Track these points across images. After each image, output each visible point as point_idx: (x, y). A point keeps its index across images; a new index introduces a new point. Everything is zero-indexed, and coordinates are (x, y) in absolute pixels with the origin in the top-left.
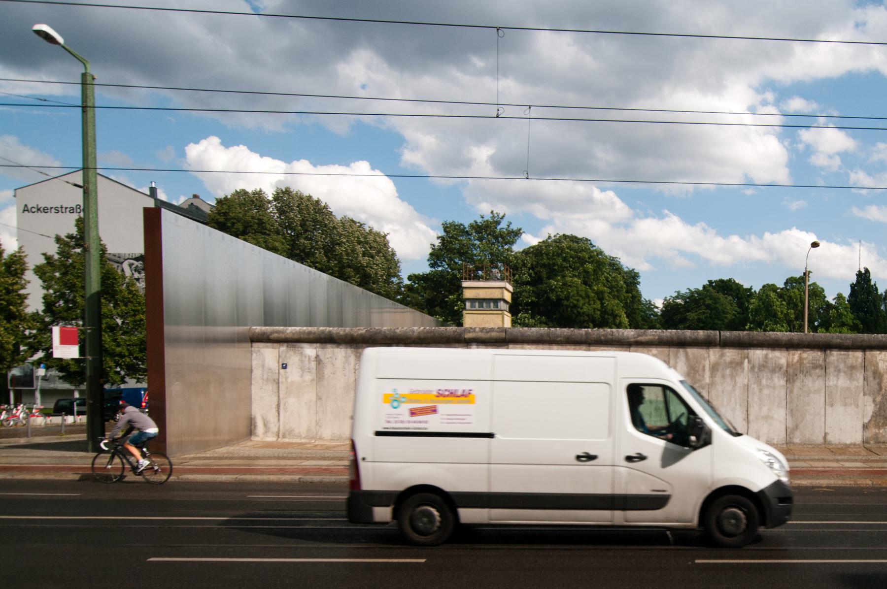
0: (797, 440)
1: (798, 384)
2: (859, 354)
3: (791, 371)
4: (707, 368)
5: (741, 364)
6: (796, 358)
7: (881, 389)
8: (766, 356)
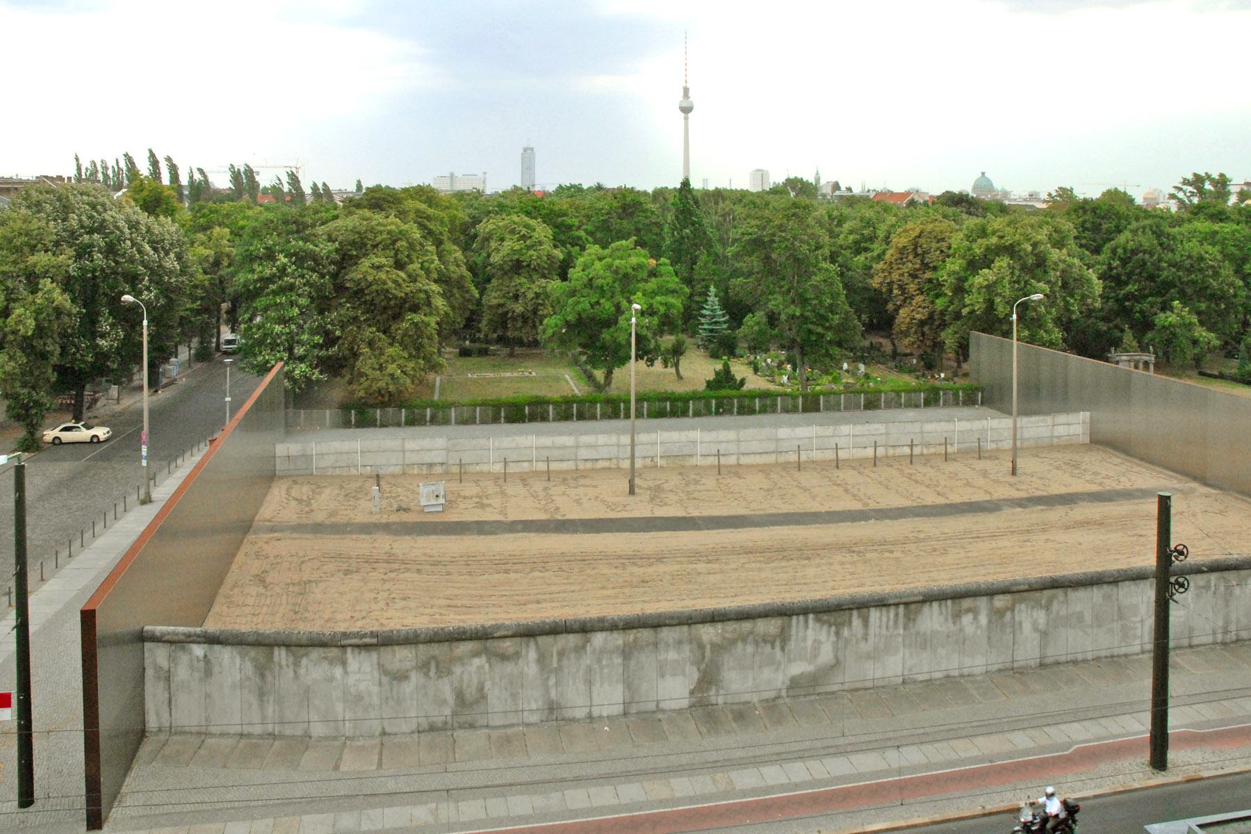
1: (633, 663)
3: (627, 649)
5: (584, 647)
6: (632, 637)
7: (704, 658)
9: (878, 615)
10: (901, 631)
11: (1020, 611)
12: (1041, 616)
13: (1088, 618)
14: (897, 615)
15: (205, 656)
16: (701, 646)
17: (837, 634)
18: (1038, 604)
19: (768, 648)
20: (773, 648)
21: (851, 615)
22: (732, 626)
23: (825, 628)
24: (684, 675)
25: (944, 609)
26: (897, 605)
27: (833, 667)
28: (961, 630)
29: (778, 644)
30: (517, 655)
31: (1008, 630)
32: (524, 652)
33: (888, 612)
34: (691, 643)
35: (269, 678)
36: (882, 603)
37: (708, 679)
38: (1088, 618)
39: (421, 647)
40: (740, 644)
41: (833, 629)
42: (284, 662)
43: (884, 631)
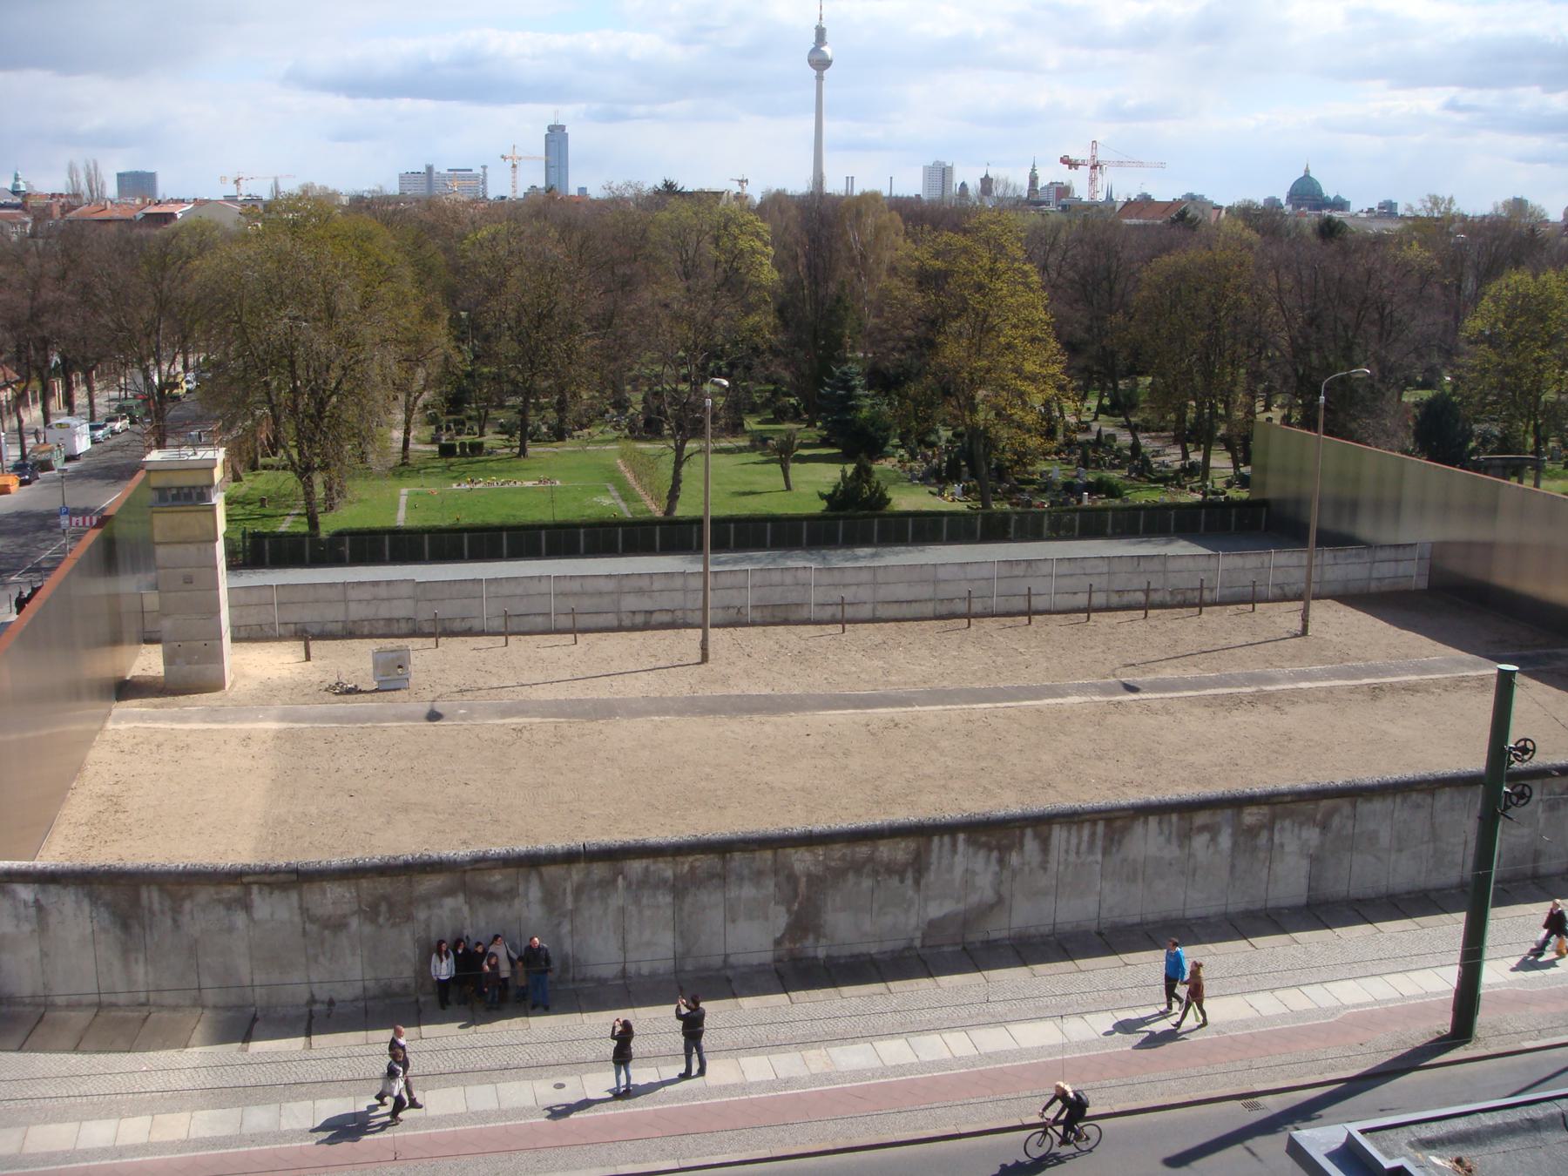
0: (689, 967)
1: (689, 899)
2: (768, 854)
4: (569, 890)
5: (615, 880)
6: (686, 867)
7: (796, 895)
8: (647, 868)
9: (1064, 834)
10: (1099, 857)
11: (1282, 829)
12: (1312, 835)
13: (1385, 837)
14: (1093, 834)
15: (37, 901)
16: (792, 878)
17: (1001, 861)
18: (1310, 820)
19: (894, 881)
20: (902, 881)
21: (1023, 836)
22: (838, 851)
23: (982, 853)
24: (766, 918)
25: (1165, 827)
26: (1094, 822)
27: (991, 907)
28: (1190, 855)
29: (909, 875)
30: (511, 894)
31: (1262, 855)
32: (521, 889)
33: (1079, 831)
34: (776, 873)
35: (136, 930)
36: (1072, 818)
37: (804, 923)
38: (1385, 837)
39: (364, 883)
40: (851, 877)
41: (995, 854)
42: (156, 907)
43: (1072, 858)
